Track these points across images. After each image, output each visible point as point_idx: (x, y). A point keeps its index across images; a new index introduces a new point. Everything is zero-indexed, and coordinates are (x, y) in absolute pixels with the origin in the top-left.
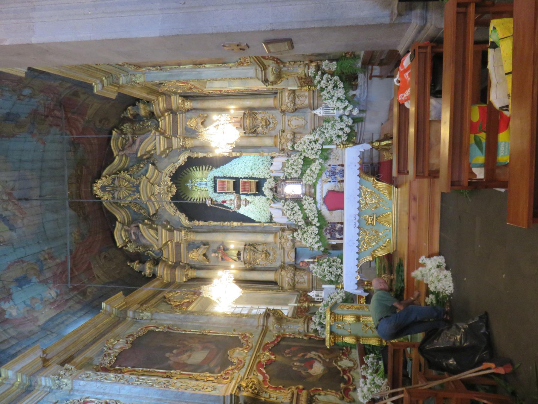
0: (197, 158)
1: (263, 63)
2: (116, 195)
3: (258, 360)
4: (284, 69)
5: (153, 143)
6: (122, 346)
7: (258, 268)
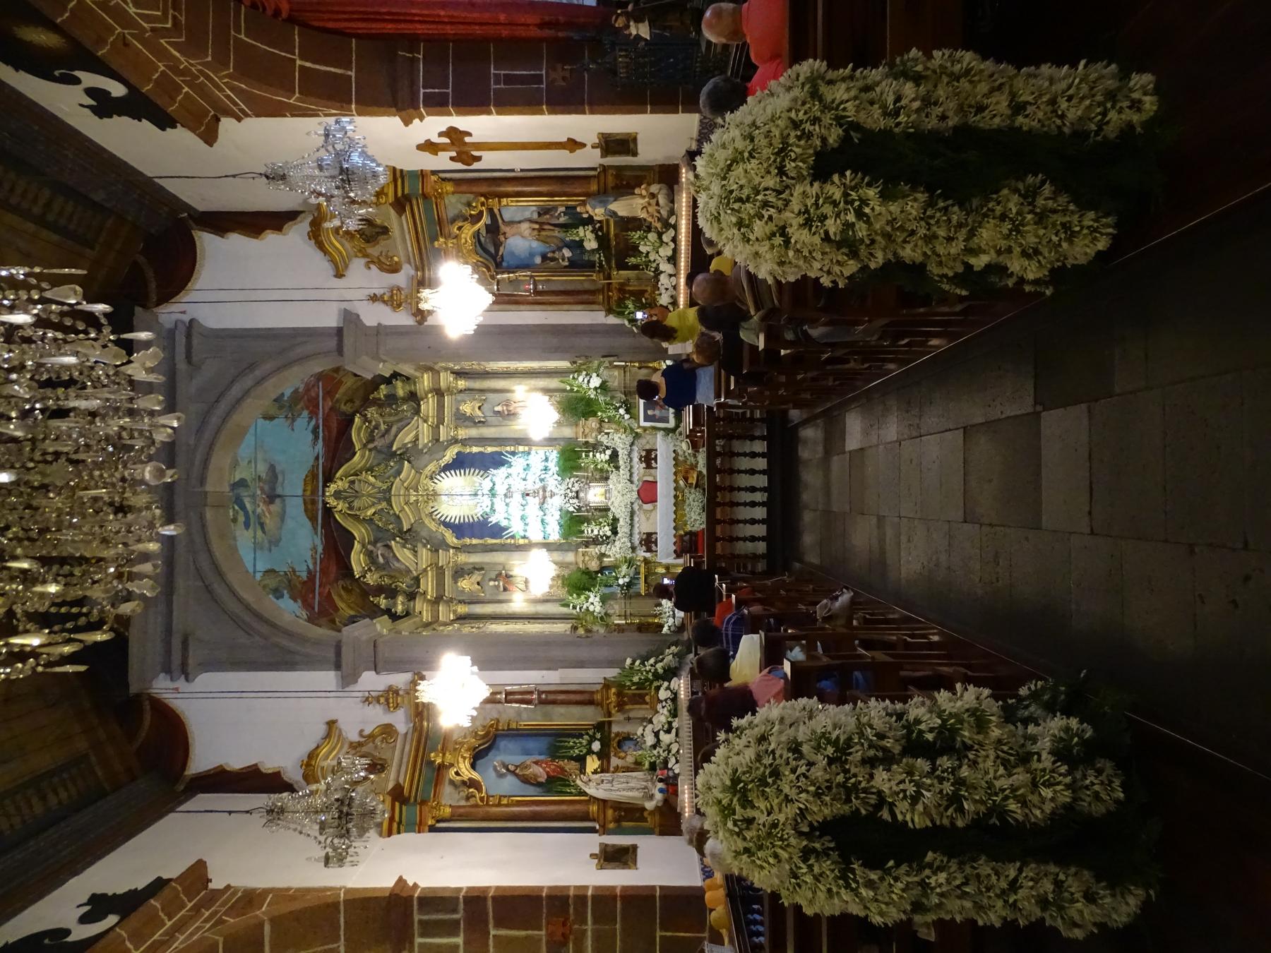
0: (470, 453)
2: (356, 504)
5: (418, 431)
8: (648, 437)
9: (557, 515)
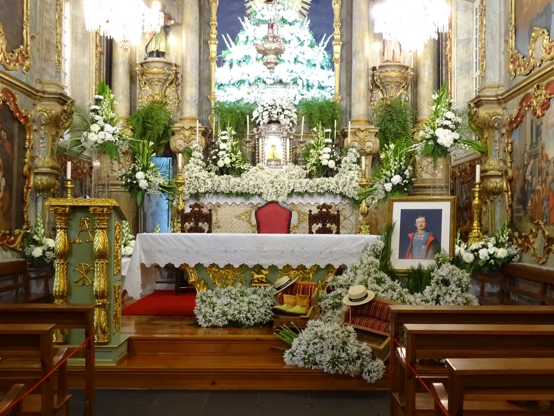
1: (513, 98)
4: (497, 135)
7: (134, 88)
8: (353, 219)
9: (251, 99)
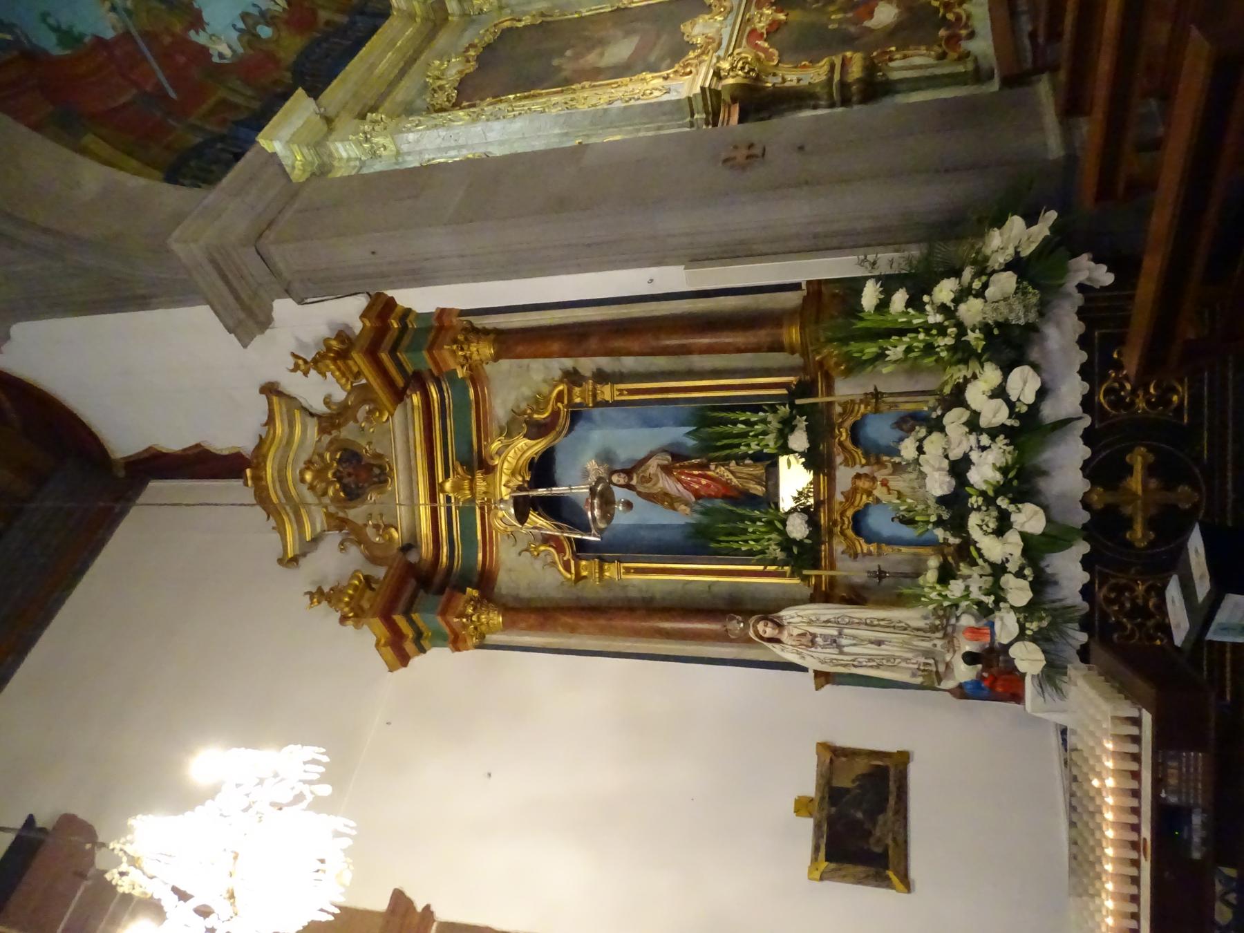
3: (748, 29)
6: (460, 68)
